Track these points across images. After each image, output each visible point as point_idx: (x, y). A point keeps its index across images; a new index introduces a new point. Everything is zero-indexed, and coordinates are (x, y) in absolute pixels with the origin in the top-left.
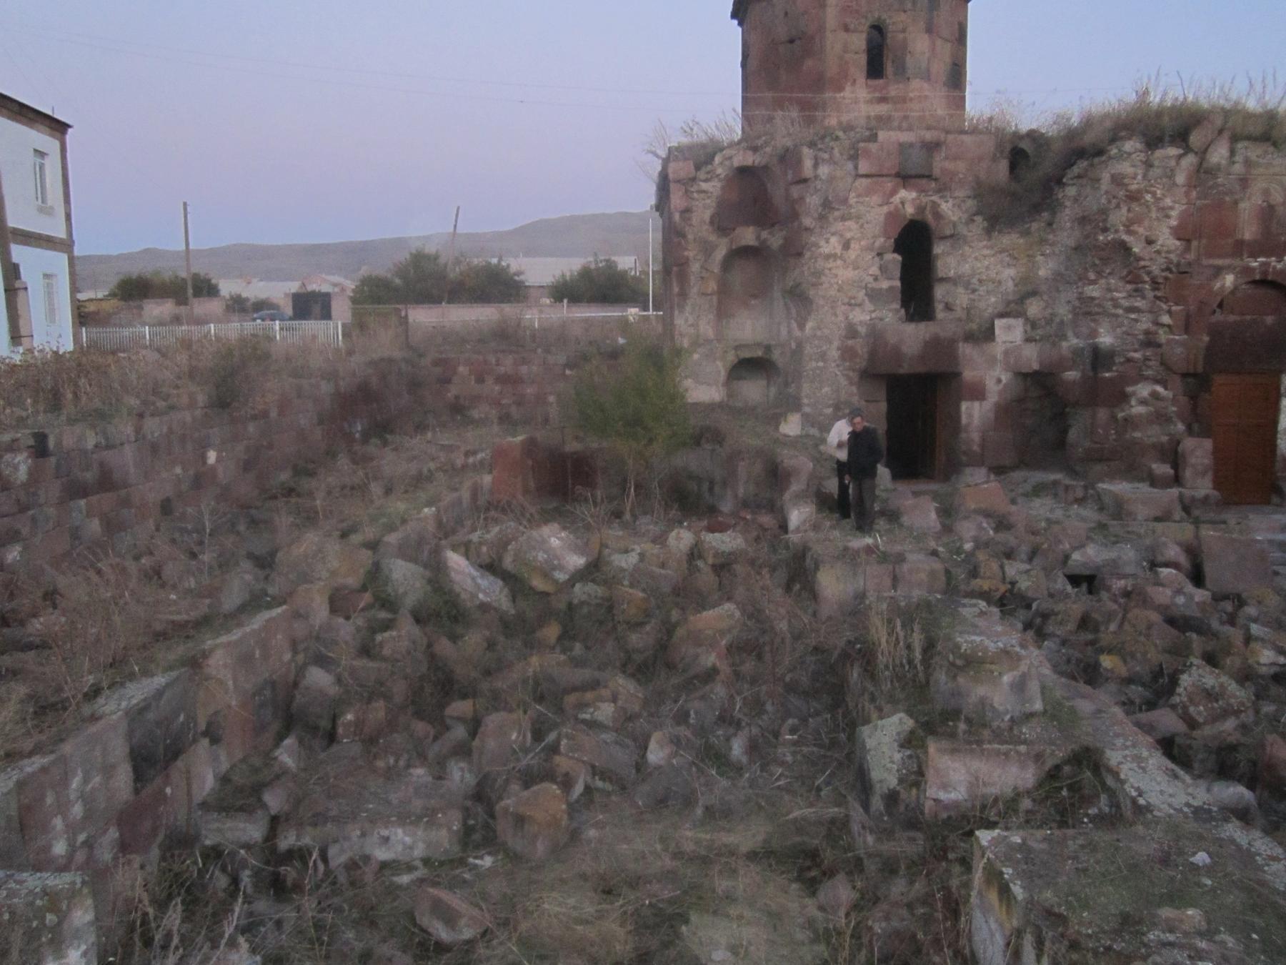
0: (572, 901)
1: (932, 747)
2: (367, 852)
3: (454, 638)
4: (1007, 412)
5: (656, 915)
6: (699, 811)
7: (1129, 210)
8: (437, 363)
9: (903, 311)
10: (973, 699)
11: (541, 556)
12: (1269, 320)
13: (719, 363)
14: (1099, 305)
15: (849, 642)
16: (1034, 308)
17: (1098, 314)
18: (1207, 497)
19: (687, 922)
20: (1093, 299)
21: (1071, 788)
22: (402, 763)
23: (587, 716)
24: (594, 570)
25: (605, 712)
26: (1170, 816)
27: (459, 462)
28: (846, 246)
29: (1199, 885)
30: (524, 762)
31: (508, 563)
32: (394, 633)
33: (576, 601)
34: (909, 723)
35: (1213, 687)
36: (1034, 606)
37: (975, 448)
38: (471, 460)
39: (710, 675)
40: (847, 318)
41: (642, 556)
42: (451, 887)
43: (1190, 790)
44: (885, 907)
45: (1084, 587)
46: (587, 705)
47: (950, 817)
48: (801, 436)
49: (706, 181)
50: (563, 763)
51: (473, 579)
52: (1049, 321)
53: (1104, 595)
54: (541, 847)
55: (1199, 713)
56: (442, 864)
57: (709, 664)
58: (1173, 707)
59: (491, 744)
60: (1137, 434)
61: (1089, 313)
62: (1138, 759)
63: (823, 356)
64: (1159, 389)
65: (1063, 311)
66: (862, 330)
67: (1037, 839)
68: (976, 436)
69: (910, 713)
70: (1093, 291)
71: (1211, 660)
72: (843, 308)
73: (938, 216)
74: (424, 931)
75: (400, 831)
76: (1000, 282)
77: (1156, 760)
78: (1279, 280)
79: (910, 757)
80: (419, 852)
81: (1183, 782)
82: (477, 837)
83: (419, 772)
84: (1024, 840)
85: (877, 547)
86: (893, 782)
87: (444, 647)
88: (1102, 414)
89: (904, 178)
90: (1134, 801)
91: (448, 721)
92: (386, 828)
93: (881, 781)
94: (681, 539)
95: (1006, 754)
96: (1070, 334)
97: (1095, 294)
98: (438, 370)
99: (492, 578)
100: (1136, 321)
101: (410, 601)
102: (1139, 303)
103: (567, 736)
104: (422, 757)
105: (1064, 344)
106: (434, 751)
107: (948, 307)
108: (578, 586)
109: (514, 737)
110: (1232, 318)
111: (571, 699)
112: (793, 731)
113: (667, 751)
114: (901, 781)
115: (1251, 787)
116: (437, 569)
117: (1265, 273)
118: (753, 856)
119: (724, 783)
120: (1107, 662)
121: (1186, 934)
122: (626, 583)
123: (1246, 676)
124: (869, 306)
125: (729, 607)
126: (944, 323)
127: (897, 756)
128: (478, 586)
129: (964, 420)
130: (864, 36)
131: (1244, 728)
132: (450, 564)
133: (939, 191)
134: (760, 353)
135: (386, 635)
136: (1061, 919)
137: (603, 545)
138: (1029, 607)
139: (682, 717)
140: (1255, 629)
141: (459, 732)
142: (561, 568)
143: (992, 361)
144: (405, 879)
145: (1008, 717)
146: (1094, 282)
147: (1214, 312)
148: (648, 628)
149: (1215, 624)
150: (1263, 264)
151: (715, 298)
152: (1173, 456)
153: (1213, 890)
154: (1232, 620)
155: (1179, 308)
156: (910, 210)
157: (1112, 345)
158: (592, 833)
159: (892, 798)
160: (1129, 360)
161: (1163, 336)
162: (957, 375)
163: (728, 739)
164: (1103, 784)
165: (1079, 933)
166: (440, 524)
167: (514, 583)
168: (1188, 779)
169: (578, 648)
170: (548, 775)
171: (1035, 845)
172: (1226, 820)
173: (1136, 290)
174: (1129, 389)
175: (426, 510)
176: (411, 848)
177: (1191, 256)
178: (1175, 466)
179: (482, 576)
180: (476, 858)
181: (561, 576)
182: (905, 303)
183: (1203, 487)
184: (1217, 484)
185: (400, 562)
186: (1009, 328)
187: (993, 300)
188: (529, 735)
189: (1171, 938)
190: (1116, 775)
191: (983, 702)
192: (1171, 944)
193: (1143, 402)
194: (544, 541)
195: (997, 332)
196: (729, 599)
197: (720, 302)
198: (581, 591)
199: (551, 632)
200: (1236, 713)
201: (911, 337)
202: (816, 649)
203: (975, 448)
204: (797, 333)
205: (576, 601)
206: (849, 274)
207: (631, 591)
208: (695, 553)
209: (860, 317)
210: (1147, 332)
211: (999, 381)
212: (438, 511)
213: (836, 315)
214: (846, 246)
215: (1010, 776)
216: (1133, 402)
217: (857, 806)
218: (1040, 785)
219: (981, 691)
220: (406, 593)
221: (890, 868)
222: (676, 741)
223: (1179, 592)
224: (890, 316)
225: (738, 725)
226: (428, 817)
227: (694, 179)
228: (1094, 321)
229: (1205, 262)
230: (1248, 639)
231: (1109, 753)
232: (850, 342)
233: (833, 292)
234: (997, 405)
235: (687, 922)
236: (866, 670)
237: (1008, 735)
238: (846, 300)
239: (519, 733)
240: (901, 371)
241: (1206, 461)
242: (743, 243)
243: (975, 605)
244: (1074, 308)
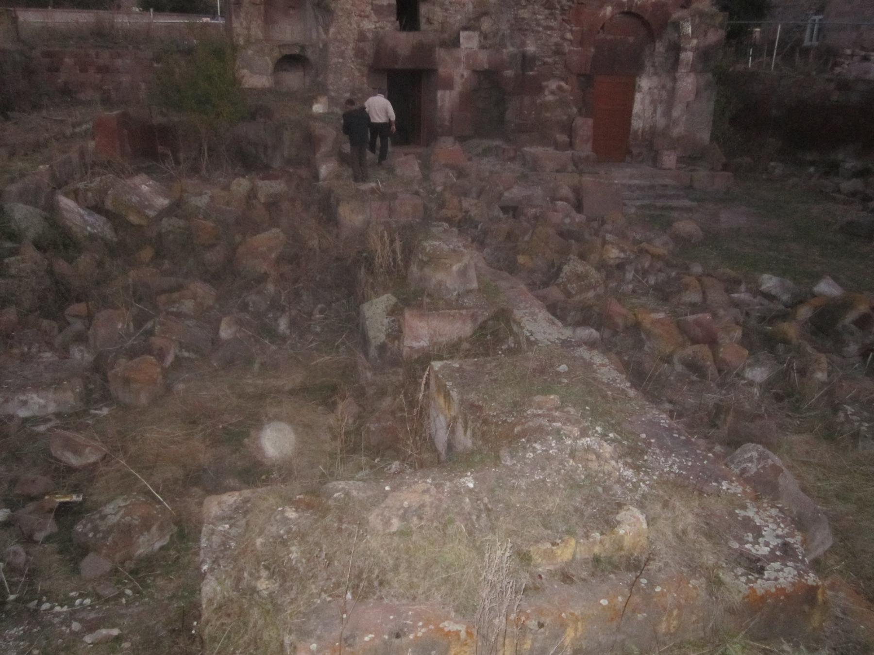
0: (167, 430)
1: (407, 314)
2: (11, 413)
3: (70, 260)
4: (467, 99)
5: (227, 434)
6: (256, 366)
8: (47, 54)
9: (398, 23)
10: (434, 281)
11: (135, 199)
12: (631, 39)
13: (268, 58)
14: (527, 24)
15: (359, 252)
16: (486, 24)
17: (527, 30)
18: (588, 157)
19: (248, 436)
20: (523, 19)
21: (492, 334)
22: (34, 350)
23: (175, 310)
24: (176, 208)
25: (188, 306)
26: (548, 346)
27: (68, 131)
29: (560, 383)
30: (130, 342)
31: (109, 204)
32: (19, 257)
33: (164, 231)
34: (393, 300)
35: (582, 272)
36: (479, 227)
37: (447, 123)
38: (77, 130)
39: (263, 278)
40: (359, 26)
41: (212, 198)
42: (78, 430)
43: (561, 330)
44: (377, 414)
45: (511, 213)
46: (174, 302)
47: (419, 358)
48: (328, 113)
50: (157, 341)
51: (82, 216)
52: (495, 34)
53: (522, 218)
54: (143, 399)
55: (573, 288)
56: (70, 416)
57: (263, 271)
58: (558, 285)
59: (102, 332)
60: (548, 115)
61: (520, 29)
62: (532, 314)
63: (342, 54)
64: (563, 84)
65: (505, 27)
66: (370, 35)
67: (469, 365)
68: (446, 115)
69: (394, 294)
70: (524, 14)
71: (582, 257)
72: (356, 18)
74: (56, 459)
75: (35, 396)
77: (543, 315)
79: (393, 321)
80: (52, 408)
81: (557, 326)
82: (96, 395)
83: (48, 356)
84: (461, 365)
85: (378, 189)
86: (382, 337)
87: (61, 266)
88: (527, 100)
90: (528, 339)
91: (70, 319)
92: (24, 394)
93: (375, 338)
94: (241, 185)
95: (453, 316)
96: (508, 44)
97: (526, 16)
98: (48, 60)
99: (96, 216)
100: (550, 36)
101: (31, 234)
102: (553, 23)
103: (162, 324)
104: (50, 346)
105: (504, 51)
106: (58, 340)
107: (429, 21)
108: (165, 222)
109: (120, 326)
110: (609, 37)
111: (163, 298)
112: (321, 311)
113: (234, 329)
114: (388, 336)
115: (597, 330)
116: (52, 208)
117: (631, 7)
118: (293, 392)
119: (274, 347)
120: (521, 259)
121: (550, 410)
122: (201, 216)
123: (602, 266)
124: (374, 18)
125: (274, 230)
126: (427, 33)
127: (386, 321)
128: (85, 221)
129: (439, 104)
131: (598, 297)
132: (62, 204)
134: (297, 51)
135: (12, 259)
136: (480, 408)
137: (183, 191)
138: (476, 227)
139: (244, 307)
140: (609, 237)
141: (78, 325)
142: (150, 207)
143: (458, 61)
144: (42, 428)
145: (455, 293)
146: (525, 7)
147: (599, 32)
148: (218, 248)
149: (587, 236)
151: (262, 7)
152: (569, 129)
153: (567, 384)
154: (596, 234)
155: (577, 28)
157: (535, 52)
158: (181, 386)
159: (382, 348)
160: (545, 63)
161: (567, 48)
162: (435, 71)
163: (276, 320)
164: (511, 330)
165: (489, 415)
166: (53, 177)
167: (113, 217)
168: (560, 324)
169: (167, 264)
170: (149, 351)
171: (468, 368)
172: (580, 346)
173: (551, 14)
174: (544, 84)
175: (41, 167)
176: (45, 406)
178: (570, 137)
179: (89, 214)
180: (95, 409)
181: (152, 213)
182: (400, 16)
183: (585, 150)
184: (595, 149)
185: (21, 205)
186: (469, 38)
187: (459, 17)
188: (131, 324)
189: (540, 412)
190: (519, 324)
191: (440, 283)
192: (539, 415)
193: (552, 93)
194: (136, 187)
195: (462, 40)
196: (278, 226)
197: (266, 11)
198: (167, 224)
199: (147, 254)
200: (595, 288)
201: (404, 42)
202: (337, 259)
203: (447, 123)
204: (324, 36)
205: (164, 231)
207: (203, 222)
208: (252, 194)
209: (368, 25)
210: (556, 44)
211: (462, 76)
212: (51, 166)
215: (455, 328)
216: (546, 93)
217: (362, 355)
218: (474, 333)
219: (440, 276)
220: (27, 228)
221: (382, 393)
222: (240, 323)
223: (567, 215)
224: (389, 25)
225: (283, 310)
226: (57, 384)
228: (525, 35)
230: (604, 243)
231: (515, 311)
232: (361, 44)
233: (349, 7)
234: (462, 95)
235: (248, 436)
236: (369, 270)
237: (455, 305)
239: (124, 323)
240: (397, 67)
243: (438, 226)
244: (512, 25)
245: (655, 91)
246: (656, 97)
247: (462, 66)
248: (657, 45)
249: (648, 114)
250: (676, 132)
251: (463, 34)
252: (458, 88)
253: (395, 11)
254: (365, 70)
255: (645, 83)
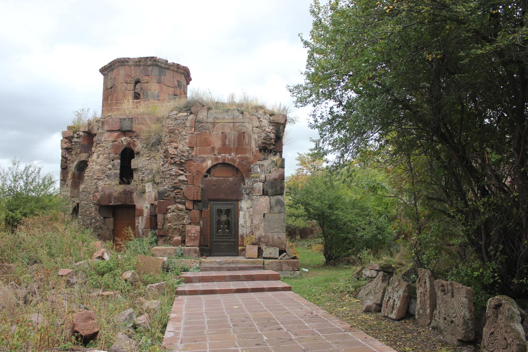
7: (170, 137)
12: (231, 179)
28: (98, 157)
49: (77, 138)
64: (180, 206)
73: (135, 146)
76: (152, 169)
78: (230, 163)
89: (124, 132)
110: (215, 179)
124: (106, 179)
129: (136, 225)
130: (133, 84)
133: (136, 136)
147: (206, 176)
150: (223, 156)
152: (183, 233)
156: (125, 143)
162: (134, 206)
174: (168, 207)
177: (194, 154)
193: (173, 212)
195: (147, 188)
206: (98, 167)
211: (147, 207)
213: (92, 183)
214: (98, 157)
227: (73, 137)
229: (199, 156)
233: (91, 174)
234: (147, 218)
238: (96, 177)
240: (111, 204)
241: (196, 235)
242: (82, 159)
245: (251, 209)
246: (252, 213)
247: (147, 202)
248: (246, 181)
249: (249, 224)
250: (258, 233)
251: (147, 185)
252: (145, 215)
253: (119, 176)
254: (98, 207)
255: (244, 204)
